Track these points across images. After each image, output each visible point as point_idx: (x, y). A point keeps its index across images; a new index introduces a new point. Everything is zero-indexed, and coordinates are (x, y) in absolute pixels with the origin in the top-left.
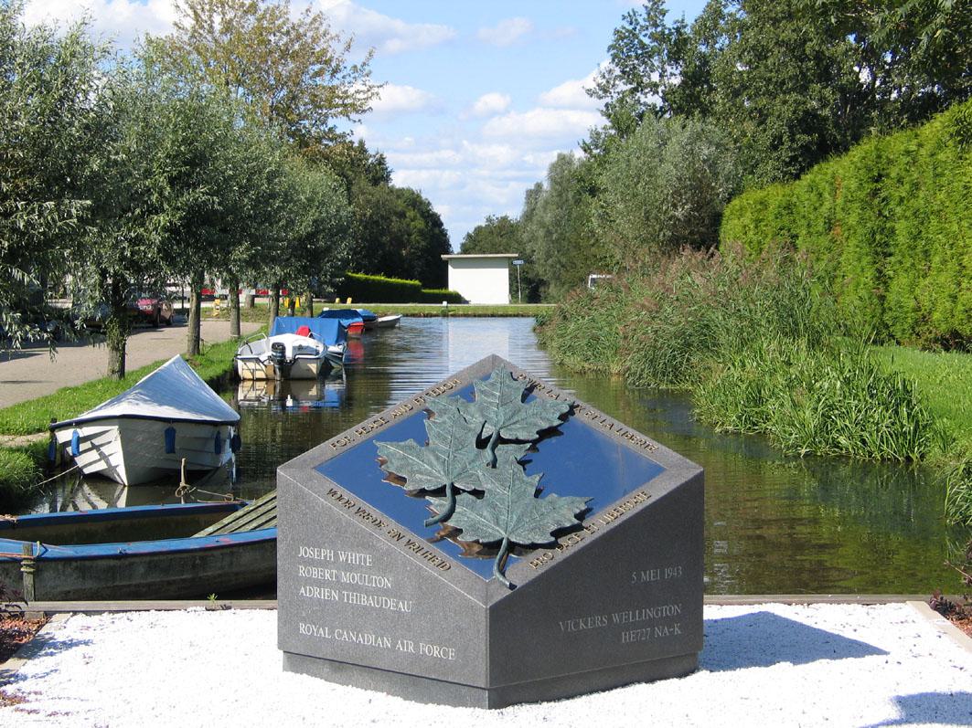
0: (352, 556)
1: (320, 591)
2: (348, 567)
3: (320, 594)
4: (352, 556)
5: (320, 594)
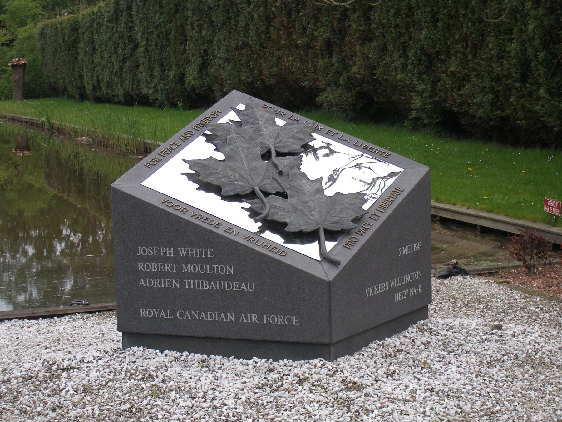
0: (192, 250)
1: (161, 281)
2: (187, 260)
3: (160, 283)
4: (192, 250)
5: (160, 283)
